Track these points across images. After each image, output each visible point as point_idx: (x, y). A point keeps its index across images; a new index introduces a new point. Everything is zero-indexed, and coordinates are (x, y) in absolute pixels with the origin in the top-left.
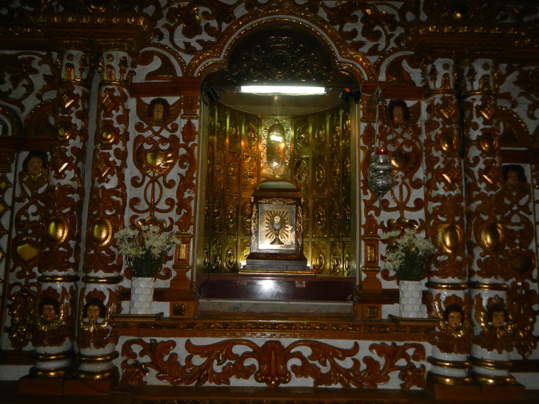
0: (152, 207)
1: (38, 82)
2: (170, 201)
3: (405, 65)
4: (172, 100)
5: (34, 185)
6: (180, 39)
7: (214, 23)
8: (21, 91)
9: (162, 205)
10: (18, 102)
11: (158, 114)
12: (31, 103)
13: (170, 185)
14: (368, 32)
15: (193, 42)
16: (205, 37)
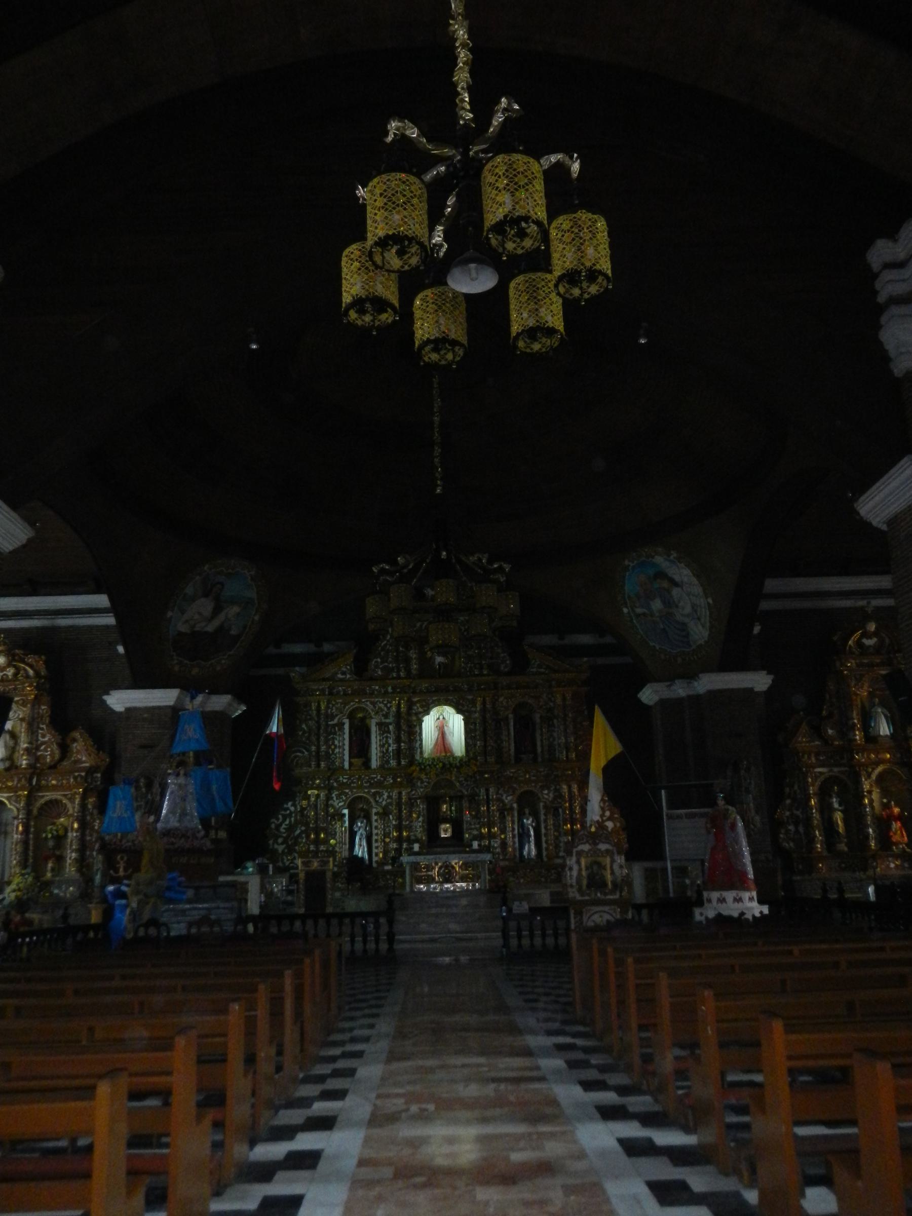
0: (416, 827)
1: (385, 797)
2: (420, 826)
3: (475, 789)
4: (418, 801)
5: (387, 823)
6: (419, 784)
7: (427, 780)
8: (381, 800)
9: (418, 827)
10: (381, 803)
11: (415, 804)
12: (384, 803)
13: (420, 822)
14: (466, 780)
15: (423, 785)
16: (425, 784)
